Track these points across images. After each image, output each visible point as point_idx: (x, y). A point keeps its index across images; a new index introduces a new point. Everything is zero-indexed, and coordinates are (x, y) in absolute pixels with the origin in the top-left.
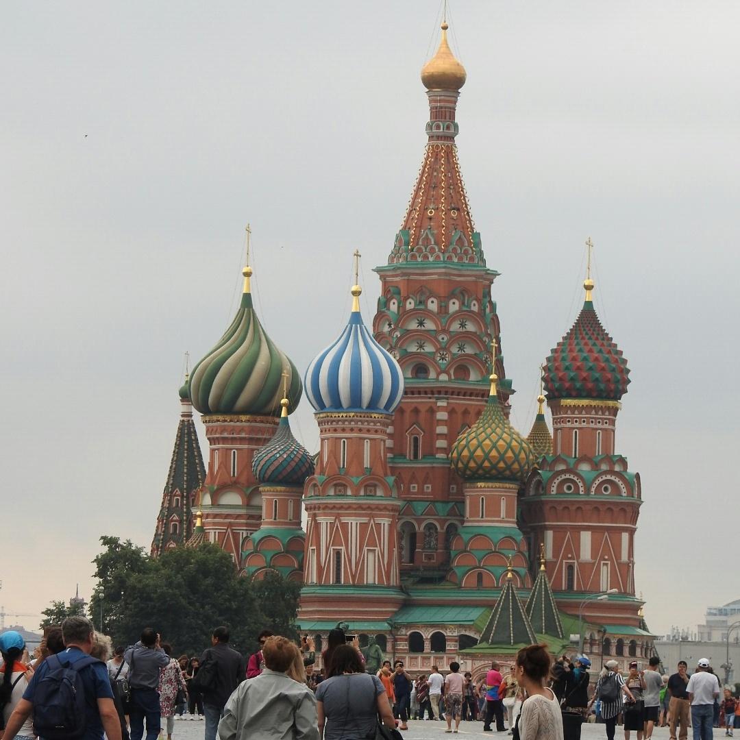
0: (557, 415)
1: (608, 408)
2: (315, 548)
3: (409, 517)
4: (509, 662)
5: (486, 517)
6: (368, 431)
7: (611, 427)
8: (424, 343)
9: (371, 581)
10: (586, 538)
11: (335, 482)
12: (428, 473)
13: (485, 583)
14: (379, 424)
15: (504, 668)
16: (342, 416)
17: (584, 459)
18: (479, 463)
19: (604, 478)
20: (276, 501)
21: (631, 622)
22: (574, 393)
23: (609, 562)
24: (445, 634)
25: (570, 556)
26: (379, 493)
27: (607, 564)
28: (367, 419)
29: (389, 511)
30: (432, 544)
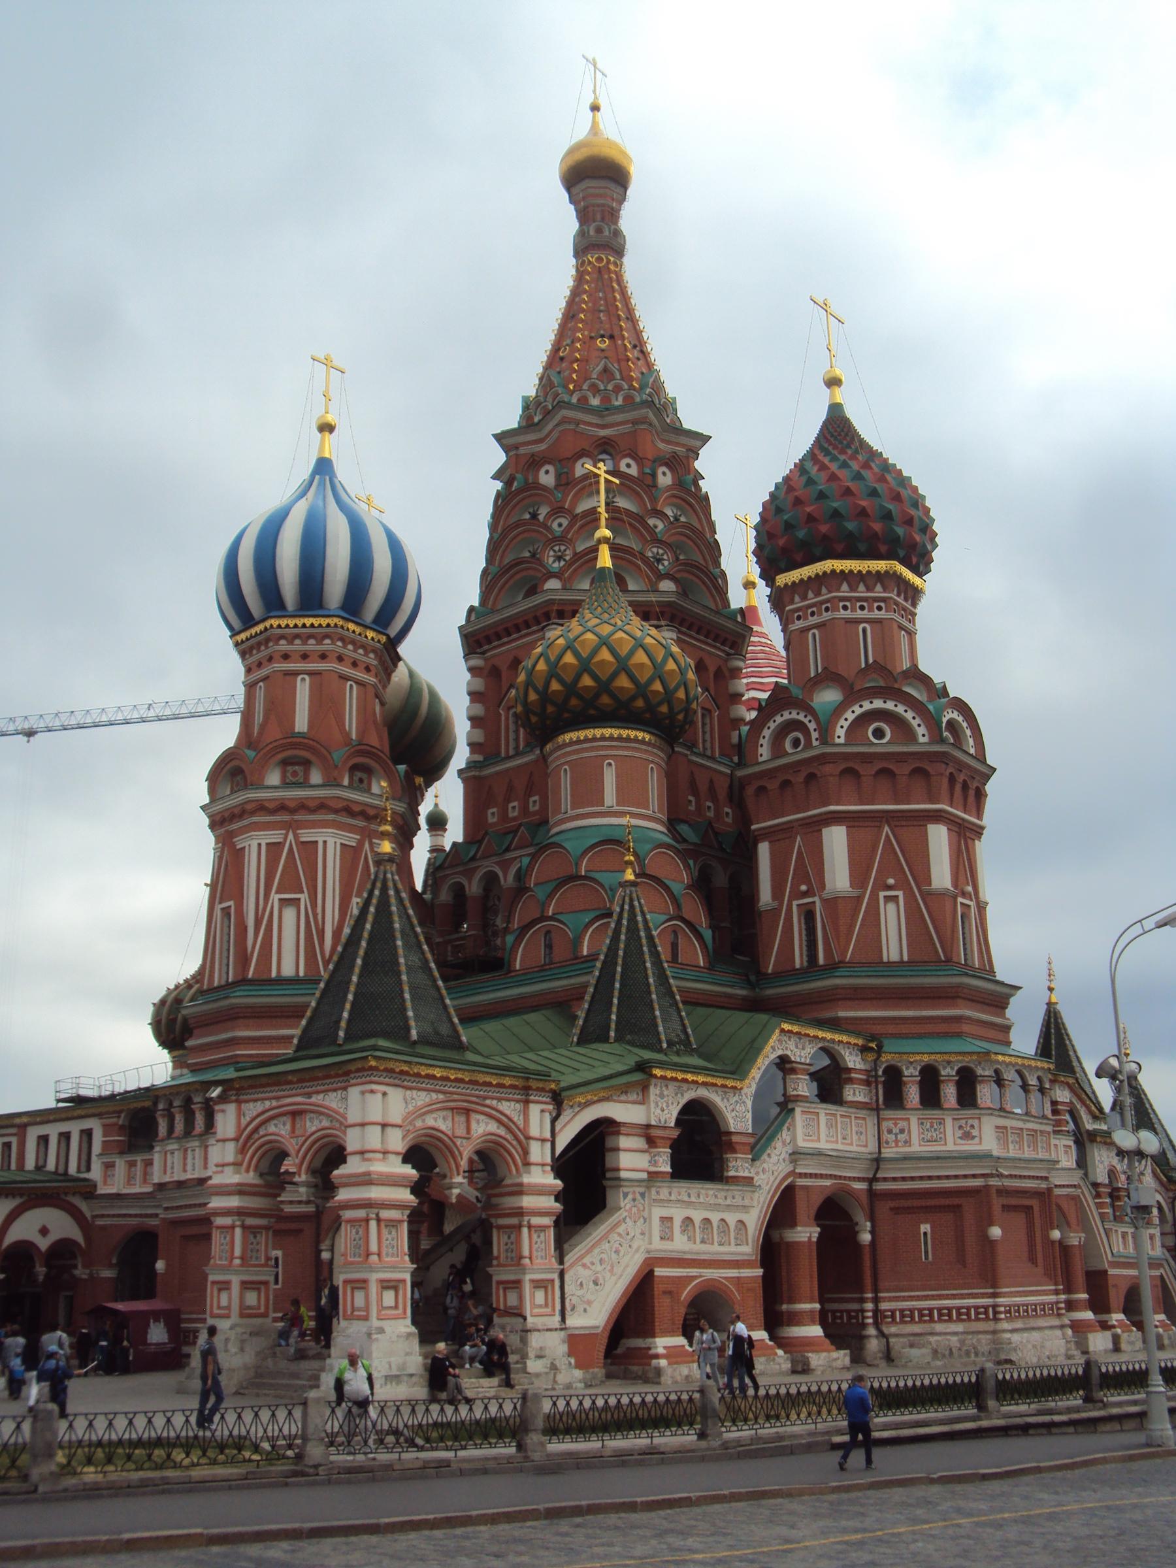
1: (880, 577)
3: (486, 863)
4: (314, 1099)
5: (572, 809)
6: (305, 657)
7: (890, 615)
9: (288, 971)
10: (836, 840)
11: (228, 767)
14: (327, 641)
15: (309, 1116)
17: (829, 677)
19: (867, 706)
21: (966, 1028)
22: (799, 557)
23: (900, 894)
25: (804, 888)
26: (316, 777)
27: (897, 897)
28: (296, 631)
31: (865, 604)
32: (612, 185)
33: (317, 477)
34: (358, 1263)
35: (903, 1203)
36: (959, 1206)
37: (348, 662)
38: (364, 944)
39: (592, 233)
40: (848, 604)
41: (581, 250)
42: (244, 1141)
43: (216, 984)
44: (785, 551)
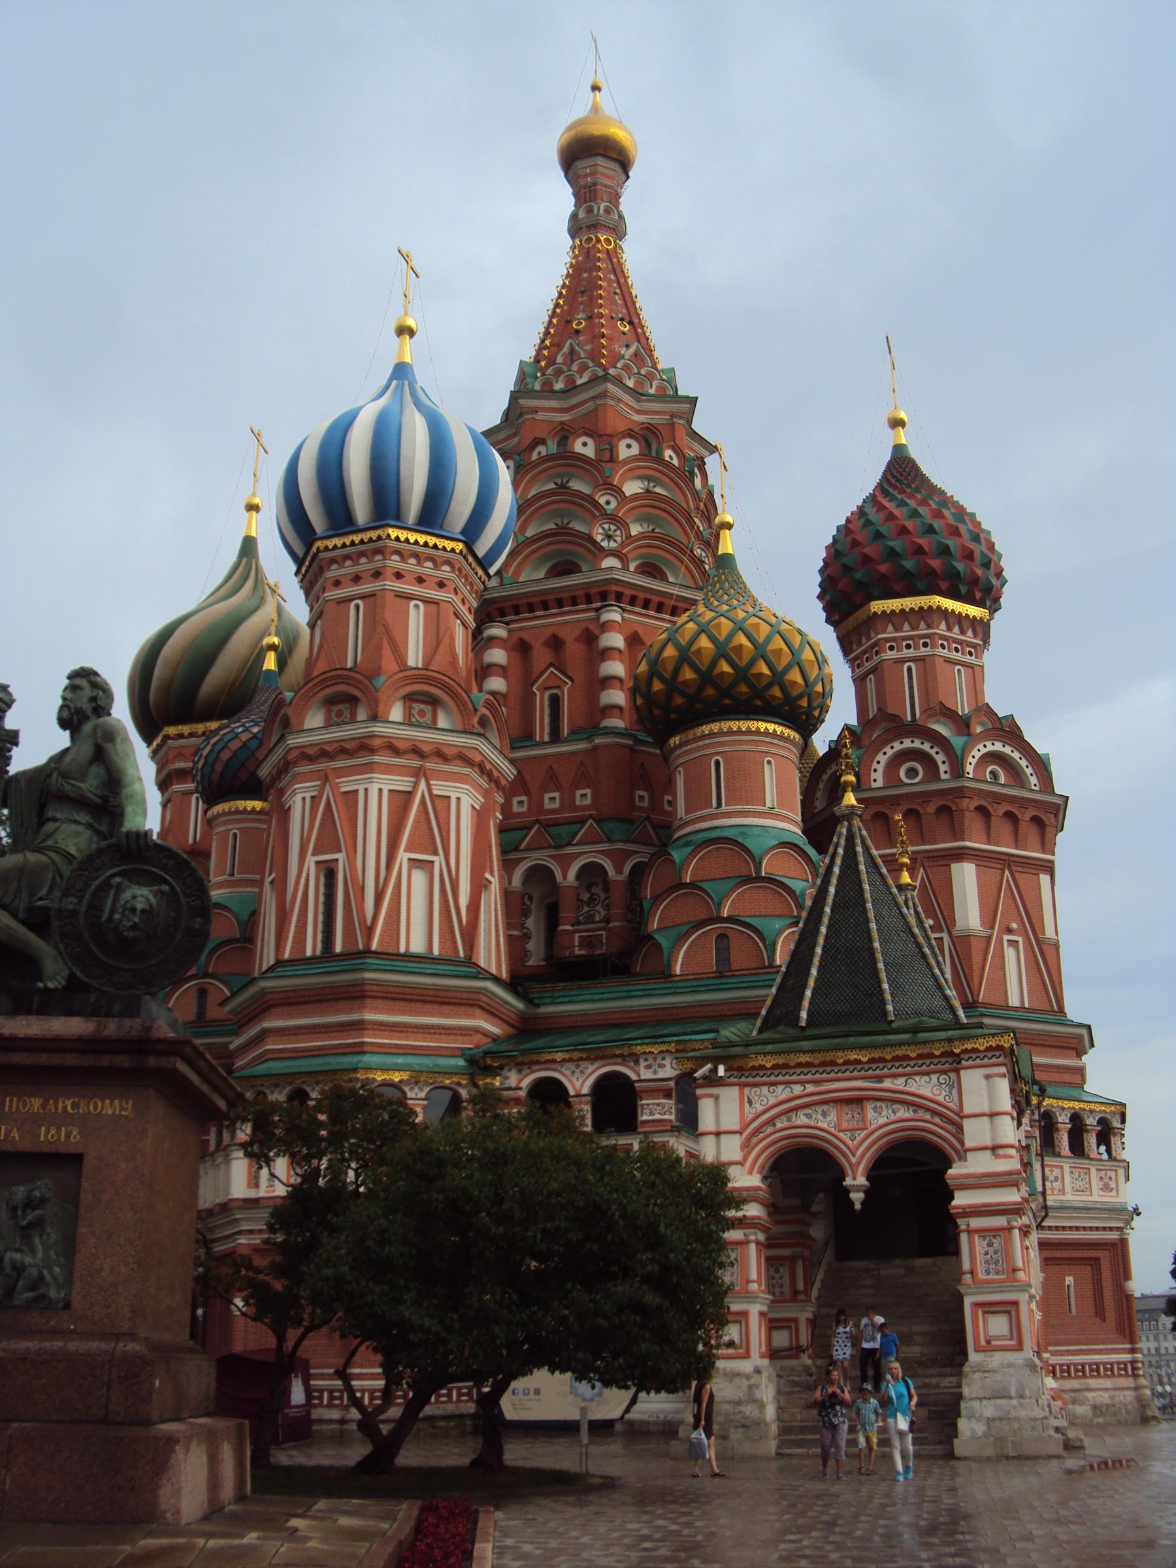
0: (860, 644)
1: (974, 622)
2: (273, 875)
3: (536, 855)
4: (887, 1084)
6: (420, 580)
8: (568, 523)
9: (417, 946)
11: (328, 691)
12: (582, 762)
13: (739, 958)
15: (869, 1107)
16: (353, 543)
18: (704, 669)
20: (235, 835)
22: (898, 587)
24: (633, 1077)
27: (1017, 942)
28: (415, 548)
29: (468, 762)
30: (597, 918)
31: (959, 647)
32: (620, 171)
33: (406, 382)
34: (1000, 1281)
35: (1057, 1254)
36: (1099, 1259)
37: (460, 596)
38: (869, 906)
39: (601, 212)
40: (945, 643)
41: (576, 228)
42: (750, 1135)
43: (309, 953)
44: (884, 577)
